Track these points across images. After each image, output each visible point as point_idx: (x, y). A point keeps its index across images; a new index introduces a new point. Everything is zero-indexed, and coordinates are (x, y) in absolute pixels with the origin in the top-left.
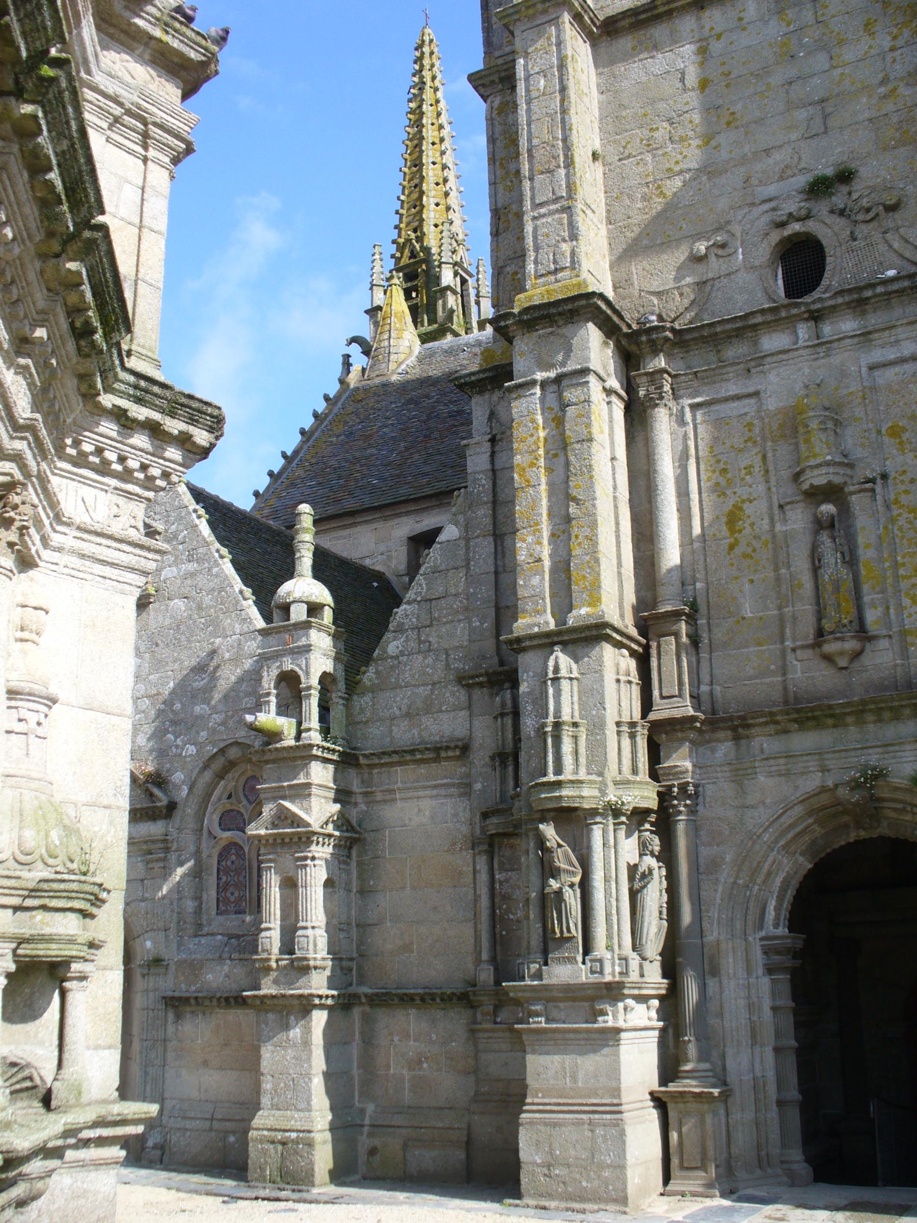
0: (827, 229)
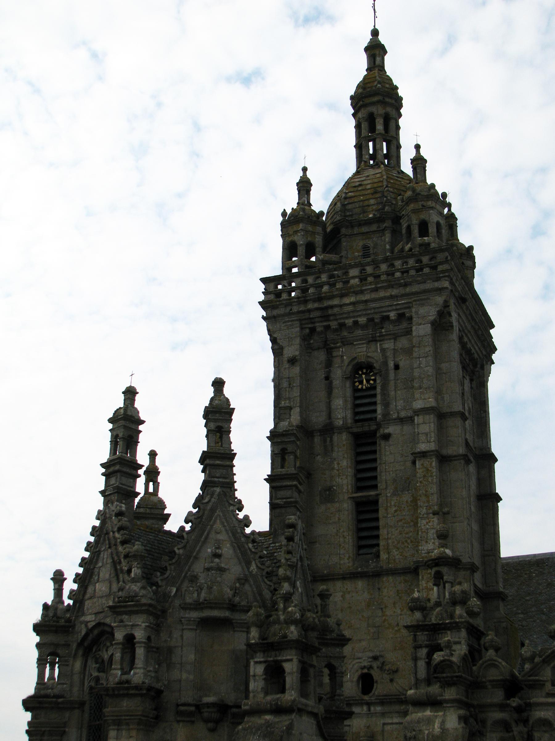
0: (375, 674)
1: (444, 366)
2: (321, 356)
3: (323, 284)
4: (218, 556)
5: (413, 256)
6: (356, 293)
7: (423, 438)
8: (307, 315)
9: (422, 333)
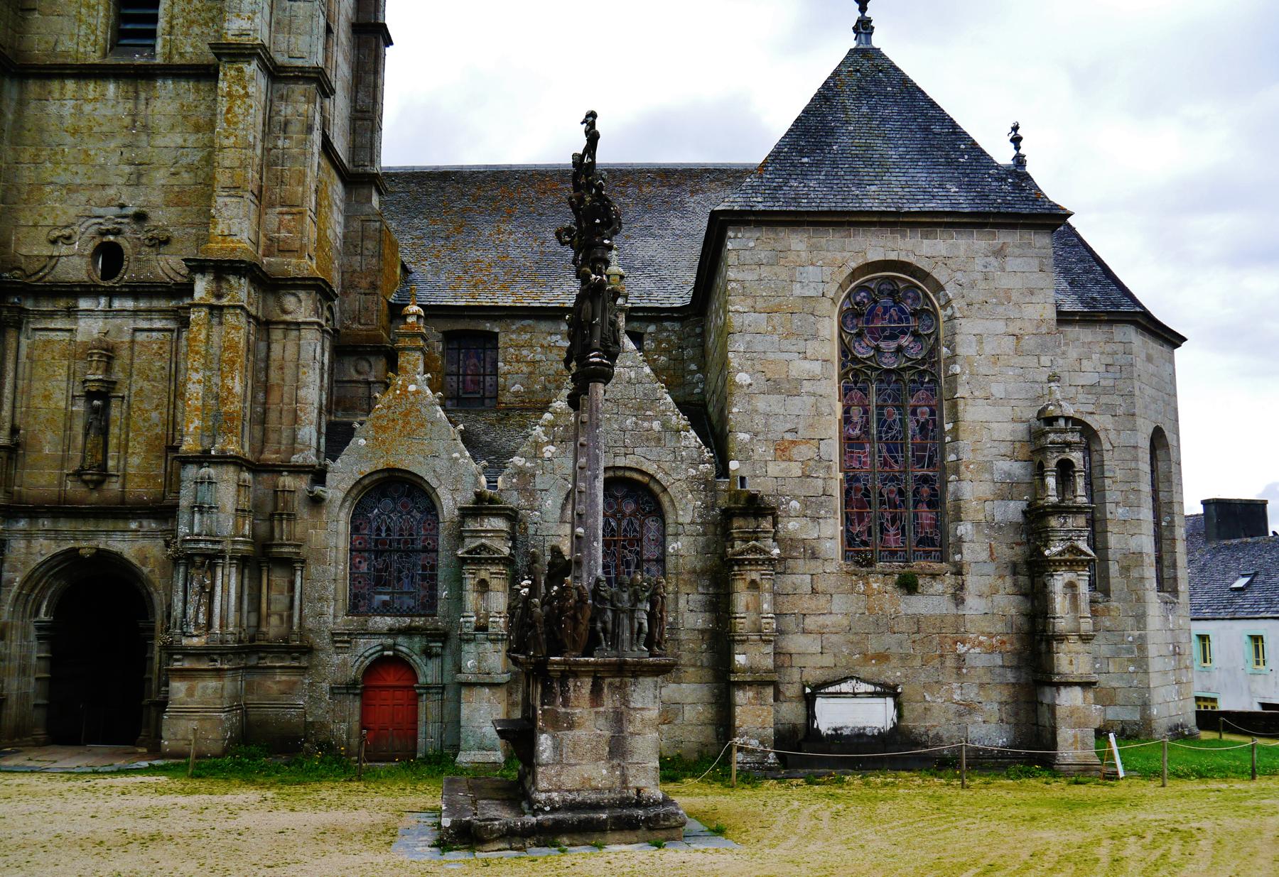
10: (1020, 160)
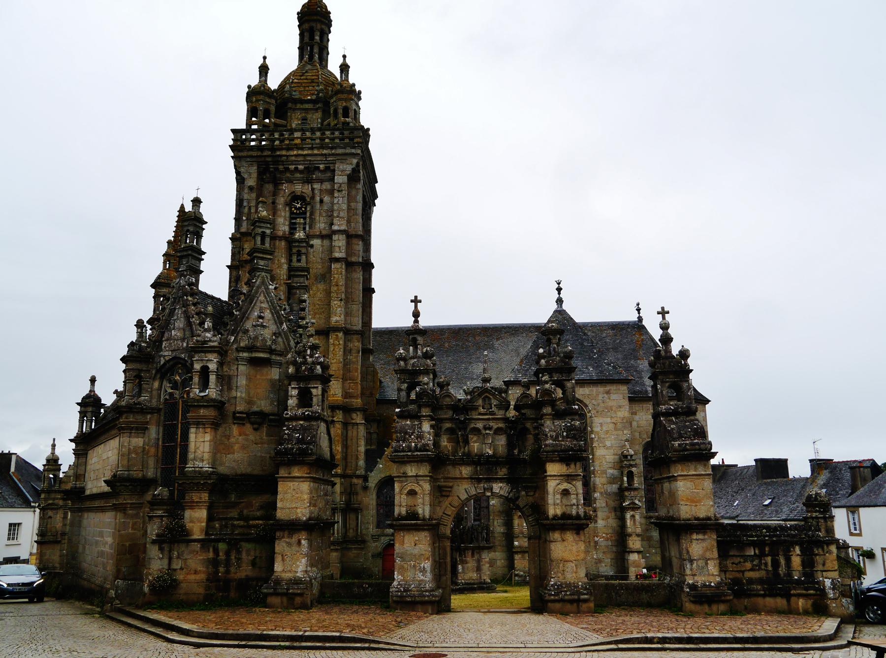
1: (352, 204)
2: (270, 187)
3: (277, 139)
4: (262, 318)
5: (338, 129)
6: (298, 149)
7: (337, 249)
8: (263, 159)
9: (341, 181)
10: (640, 319)
